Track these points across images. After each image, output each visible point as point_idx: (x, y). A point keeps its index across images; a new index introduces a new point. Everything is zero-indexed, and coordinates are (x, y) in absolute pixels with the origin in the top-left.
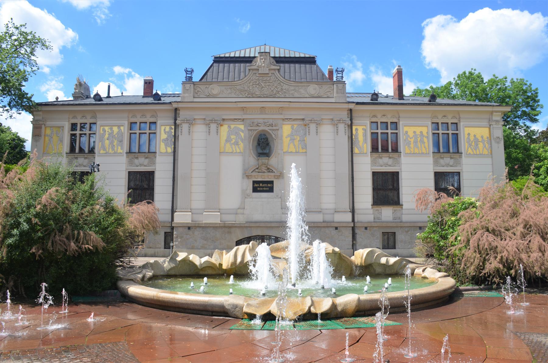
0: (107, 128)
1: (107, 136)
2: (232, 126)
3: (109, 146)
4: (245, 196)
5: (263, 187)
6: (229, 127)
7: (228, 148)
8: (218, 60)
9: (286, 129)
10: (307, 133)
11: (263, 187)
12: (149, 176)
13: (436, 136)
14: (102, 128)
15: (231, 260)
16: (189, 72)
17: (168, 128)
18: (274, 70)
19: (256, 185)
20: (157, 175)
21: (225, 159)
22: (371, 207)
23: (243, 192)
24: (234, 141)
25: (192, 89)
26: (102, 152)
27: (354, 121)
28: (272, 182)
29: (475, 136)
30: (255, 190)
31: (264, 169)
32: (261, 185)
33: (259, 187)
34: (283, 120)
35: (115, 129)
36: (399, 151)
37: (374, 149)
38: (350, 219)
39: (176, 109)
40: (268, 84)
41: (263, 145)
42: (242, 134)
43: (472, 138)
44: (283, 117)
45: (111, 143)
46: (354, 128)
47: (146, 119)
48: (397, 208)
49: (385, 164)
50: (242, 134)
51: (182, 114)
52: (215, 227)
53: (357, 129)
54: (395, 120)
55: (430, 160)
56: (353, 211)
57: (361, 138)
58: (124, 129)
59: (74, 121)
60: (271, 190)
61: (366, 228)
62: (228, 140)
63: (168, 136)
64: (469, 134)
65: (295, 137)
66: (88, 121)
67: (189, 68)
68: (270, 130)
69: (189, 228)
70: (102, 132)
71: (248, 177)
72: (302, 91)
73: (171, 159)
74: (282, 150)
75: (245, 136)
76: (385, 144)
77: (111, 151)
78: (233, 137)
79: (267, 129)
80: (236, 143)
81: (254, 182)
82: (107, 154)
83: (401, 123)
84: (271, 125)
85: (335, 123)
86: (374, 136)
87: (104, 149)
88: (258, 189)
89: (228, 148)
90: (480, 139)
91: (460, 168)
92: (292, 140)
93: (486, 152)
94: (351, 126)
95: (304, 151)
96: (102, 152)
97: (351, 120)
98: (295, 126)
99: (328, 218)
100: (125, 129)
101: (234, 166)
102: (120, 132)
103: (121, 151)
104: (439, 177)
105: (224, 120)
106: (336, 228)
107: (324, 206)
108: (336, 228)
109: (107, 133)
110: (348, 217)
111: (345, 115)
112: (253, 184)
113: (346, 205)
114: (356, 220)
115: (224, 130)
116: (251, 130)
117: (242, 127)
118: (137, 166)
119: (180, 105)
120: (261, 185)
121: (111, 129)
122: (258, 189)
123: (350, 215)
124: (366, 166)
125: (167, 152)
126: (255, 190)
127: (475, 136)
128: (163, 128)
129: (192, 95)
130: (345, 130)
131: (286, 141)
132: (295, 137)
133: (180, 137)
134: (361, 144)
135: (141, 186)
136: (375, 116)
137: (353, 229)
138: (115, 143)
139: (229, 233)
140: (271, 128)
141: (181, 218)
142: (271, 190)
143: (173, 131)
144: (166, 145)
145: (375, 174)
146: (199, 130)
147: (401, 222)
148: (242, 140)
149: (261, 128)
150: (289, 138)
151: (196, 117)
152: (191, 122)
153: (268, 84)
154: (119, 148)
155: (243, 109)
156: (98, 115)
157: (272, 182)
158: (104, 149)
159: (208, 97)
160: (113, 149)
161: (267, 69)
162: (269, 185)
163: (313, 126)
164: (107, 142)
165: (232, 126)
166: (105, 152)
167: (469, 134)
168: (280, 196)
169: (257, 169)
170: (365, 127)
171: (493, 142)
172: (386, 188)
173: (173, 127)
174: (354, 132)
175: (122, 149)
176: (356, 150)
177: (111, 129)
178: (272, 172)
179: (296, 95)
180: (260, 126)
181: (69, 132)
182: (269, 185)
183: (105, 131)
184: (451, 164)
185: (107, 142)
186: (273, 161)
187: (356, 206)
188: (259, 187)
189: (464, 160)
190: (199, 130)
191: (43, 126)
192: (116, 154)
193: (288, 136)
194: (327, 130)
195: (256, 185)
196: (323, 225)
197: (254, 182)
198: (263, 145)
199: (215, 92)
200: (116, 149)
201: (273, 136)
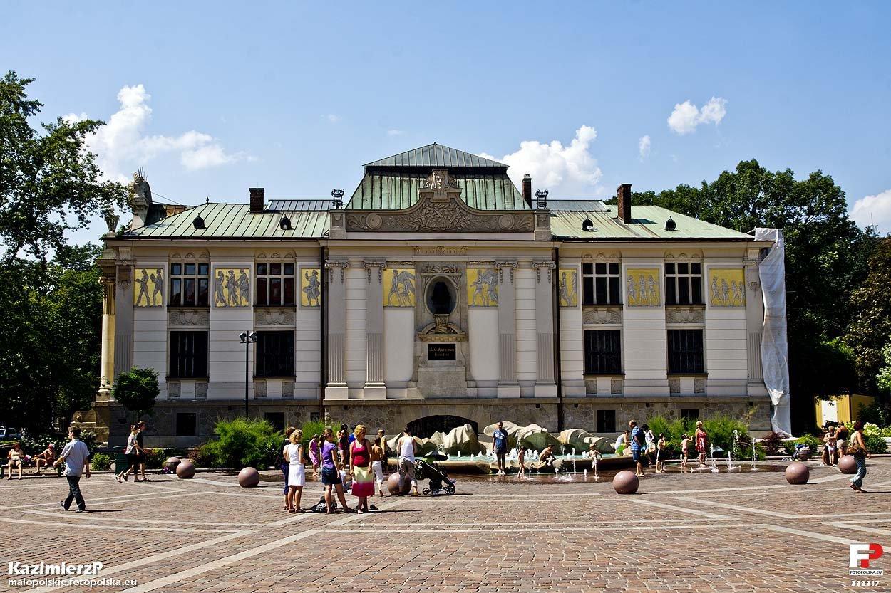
0: (224, 272)
1: (225, 282)
2: (400, 271)
3: (229, 296)
4: (417, 362)
5: (442, 352)
6: (395, 272)
7: (395, 300)
8: (371, 170)
9: (472, 274)
10: (499, 280)
11: (442, 353)
13: (670, 283)
14: (217, 271)
15: (452, 441)
17: (310, 272)
20: (299, 337)
21: (390, 314)
22: (583, 377)
23: (416, 359)
24: (402, 291)
25: (344, 220)
26: (219, 304)
27: (561, 263)
28: (453, 346)
29: (723, 281)
30: (431, 356)
31: (443, 329)
34: (467, 262)
35: (237, 273)
36: (620, 302)
37: (587, 301)
38: (555, 394)
39: (323, 248)
40: (446, 213)
41: (441, 297)
42: (413, 282)
43: (719, 283)
44: (467, 260)
45: (232, 292)
46: (561, 272)
47: (279, 259)
48: (618, 379)
49: (602, 320)
50: (413, 282)
51: (333, 255)
52: (379, 406)
54: (616, 261)
55: (661, 313)
56: (559, 383)
58: (250, 272)
59: (175, 260)
60: (452, 356)
61: (576, 405)
62: (394, 290)
63: (311, 283)
64: (715, 279)
65: (483, 285)
67: (338, 188)
69: (346, 407)
70: (217, 277)
73: (317, 314)
74: (467, 303)
75: (417, 285)
76: (602, 291)
77: (231, 303)
78: (400, 285)
79: (445, 275)
80: (406, 294)
81: (430, 346)
82: (227, 307)
83: (623, 264)
84: (452, 270)
85: (536, 266)
87: (223, 301)
89: (395, 300)
90: (730, 285)
91: (702, 325)
92: (480, 289)
93: (738, 302)
94: (556, 272)
95: (494, 304)
96: (219, 304)
97: (557, 264)
98: (483, 271)
99: (527, 392)
100: (250, 273)
101: (401, 325)
102: (244, 279)
103: (247, 304)
104: (673, 336)
105: (388, 262)
106: (538, 406)
107: (522, 377)
108: (538, 406)
109: (225, 279)
110: (552, 392)
111: (548, 256)
113: (551, 376)
114: (563, 395)
115: (388, 274)
116: (425, 277)
117: (412, 271)
118: (269, 324)
119: (330, 244)
121: (231, 273)
123: (556, 388)
124: (575, 323)
125: (310, 306)
126: (431, 356)
127: (723, 281)
128: (304, 271)
130: (549, 276)
131: (471, 290)
132: (483, 285)
133: (330, 287)
135: (274, 354)
136: (588, 255)
137: (560, 406)
138: (237, 293)
139: (399, 413)
140: (450, 274)
141: (335, 393)
142: (452, 356)
143: (319, 276)
144: (309, 296)
145: (588, 334)
146: (356, 277)
147: (622, 397)
148: (413, 290)
149: (439, 274)
150: (474, 288)
151: (350, 259)
152: (344, 266)
153: (446, 213)
154: (244, 299)
155: (414, 248)
157: (453, 346)
158: (223, 301)
160: (235, 301)
163: (506, 271)
164: (226, 292)
166: (223, 305)
167: (715, 279)
168: (464, 364)
169: (434, 328)
171: (747, 288)
172: (604, 353)
173: (319, 271)
174: (561, 278)
175: (247, 300)
176: (563, 302)
177: (231, 273)
181: (169, 277)
183: (223, 276)
184: (690, 318)
185: (226, 292)
186: (455, 316)
187: (564, 376)
189: (709, 313)
190: (356, 277)
191: (132, 267)
192: (239, 307)
193: (474, 284)
194: (526, 277)
196: (522, 401)
197: (430, 346)
198: (441, 297)
200: (239, 300)
201: (455, 285)
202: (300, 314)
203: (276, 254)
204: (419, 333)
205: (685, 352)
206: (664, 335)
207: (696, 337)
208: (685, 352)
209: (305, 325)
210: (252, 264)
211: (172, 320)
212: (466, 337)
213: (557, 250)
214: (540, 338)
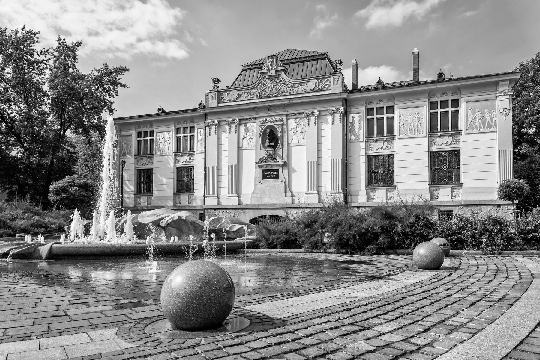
2: (248, 125)
5: (271, 175)
6: (246, 126)
11: (270, 174)
12: (190, 169)
16: (216, 82)
18: (281, 71)
19: (265, 173)
20: (196, 169)
24: (249, 137)
28: (277, 170)
30: (264, 177)
32: (269, 173)
33: (268, 175)
41: (272, 138)
44: (286, 113)
53: (353, 117)
57: (357, 125)
60: (277, 177)
66: (148, 130)
68: (276, 125)
71: (261, 166)
72: (304, 87)
79: (273, 124)
86: (370, 122)
88: (267, 176)
104: (434, 156)
112: (263, 173)
115: (242, 128)
120: (269, 173)
122: (267, 176)
126: (264, 177)
129: (216, 100)
131: (291, 133)
134: (357, 131)
141: (211, 202)
142: (277, 177)
149: (268, 124)
150: (293, 131)
156: (154, 125)
159: (230, 101)
161: (274, 71)
162: (276, 173)
165: (248, 125)
170: (361, 114)
178: (277, 161)
179: (300, 91)
180: (267, 123)
182: (276, 173)
188: (268, 175)
195: (265, 173)
198: (272, 138)
199: (235, 96)
202: (196, 156)
203: (185, 122)
204: (259, 164)
205: (445, 168)
206: (426, 156)
207: (453, 156)
208: (445, 168)
209: (198, 162)
210: (173, 128)
211: (137, 163)
212: (285, 165)
213: (346, 100)
214: (333, 162)
